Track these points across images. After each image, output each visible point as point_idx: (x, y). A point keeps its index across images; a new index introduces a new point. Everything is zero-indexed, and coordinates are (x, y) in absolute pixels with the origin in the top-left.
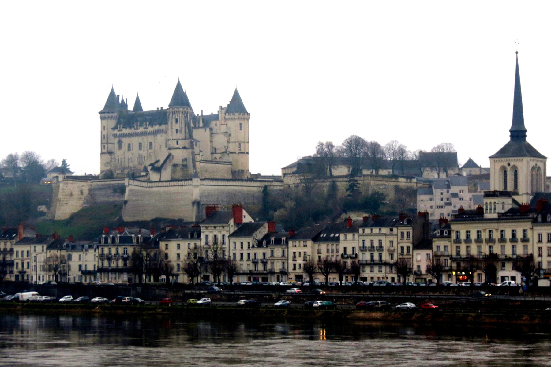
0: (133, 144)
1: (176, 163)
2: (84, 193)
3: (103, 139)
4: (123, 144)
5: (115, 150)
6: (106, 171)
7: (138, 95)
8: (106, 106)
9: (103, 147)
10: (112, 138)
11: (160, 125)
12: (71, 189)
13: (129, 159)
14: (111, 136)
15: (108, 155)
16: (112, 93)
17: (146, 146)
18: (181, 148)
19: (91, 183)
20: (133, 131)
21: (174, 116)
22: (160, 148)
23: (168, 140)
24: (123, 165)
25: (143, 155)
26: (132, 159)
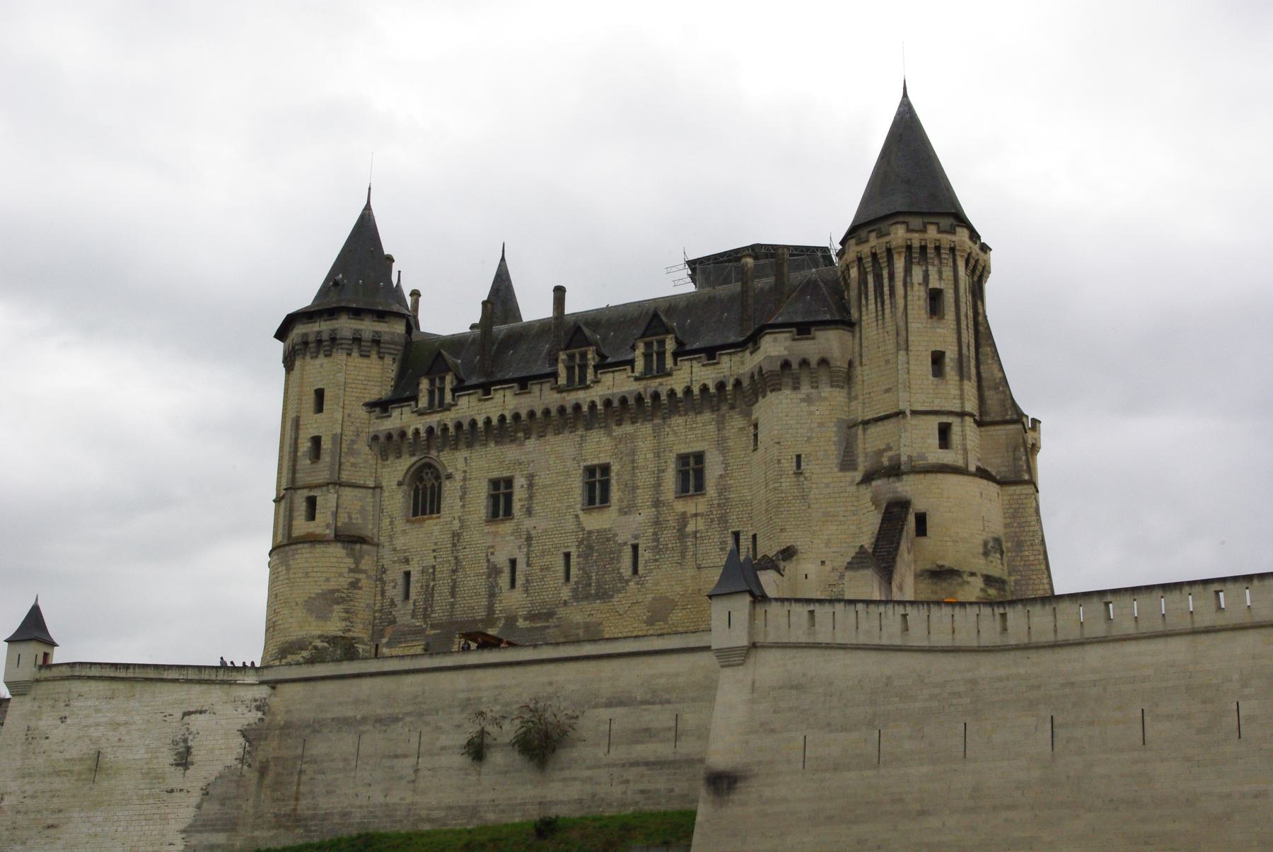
0: (531, 477)
1: (948, 563)
2: (198, 755)
3: (305, 462)
4: (450, 491)
5: (386, 522)
6: (319, 643)
7: (503, 259)
8: (332, 284)
9: (301, 507)
10: (365, 452)
11: (803, 330)
12: (94, 733)
13: (494, 571)
14: (362, 446)
15: (337, 551)
16: (365, 231)
17: (644, 479)
18: (972, 468)
19: (264, 691)
20: (543, 398)
21: (917, 273)
22: (799, 472)
23: (851, 428)
24: (439, 614)
25: (624, 536)
26: (521, 566)
